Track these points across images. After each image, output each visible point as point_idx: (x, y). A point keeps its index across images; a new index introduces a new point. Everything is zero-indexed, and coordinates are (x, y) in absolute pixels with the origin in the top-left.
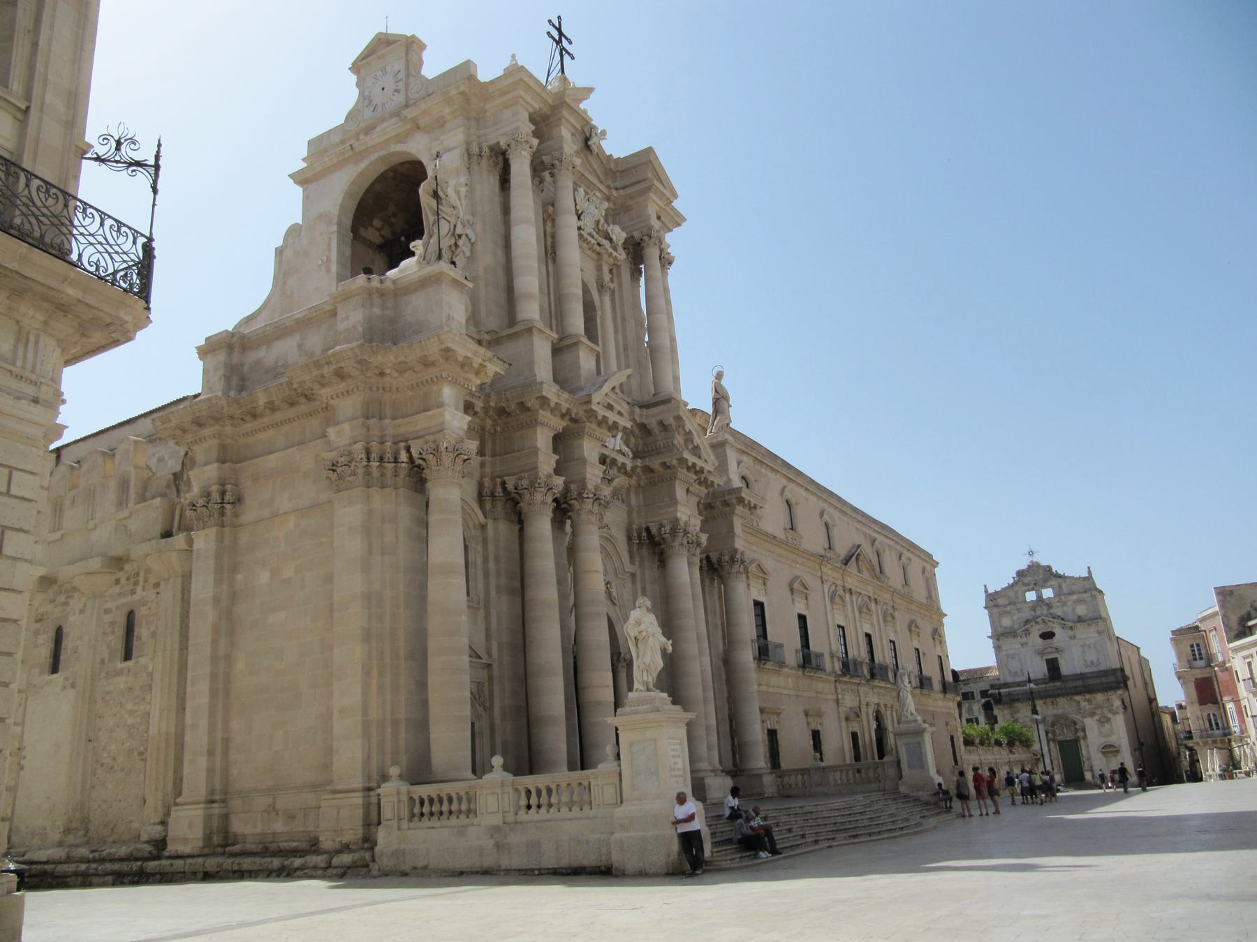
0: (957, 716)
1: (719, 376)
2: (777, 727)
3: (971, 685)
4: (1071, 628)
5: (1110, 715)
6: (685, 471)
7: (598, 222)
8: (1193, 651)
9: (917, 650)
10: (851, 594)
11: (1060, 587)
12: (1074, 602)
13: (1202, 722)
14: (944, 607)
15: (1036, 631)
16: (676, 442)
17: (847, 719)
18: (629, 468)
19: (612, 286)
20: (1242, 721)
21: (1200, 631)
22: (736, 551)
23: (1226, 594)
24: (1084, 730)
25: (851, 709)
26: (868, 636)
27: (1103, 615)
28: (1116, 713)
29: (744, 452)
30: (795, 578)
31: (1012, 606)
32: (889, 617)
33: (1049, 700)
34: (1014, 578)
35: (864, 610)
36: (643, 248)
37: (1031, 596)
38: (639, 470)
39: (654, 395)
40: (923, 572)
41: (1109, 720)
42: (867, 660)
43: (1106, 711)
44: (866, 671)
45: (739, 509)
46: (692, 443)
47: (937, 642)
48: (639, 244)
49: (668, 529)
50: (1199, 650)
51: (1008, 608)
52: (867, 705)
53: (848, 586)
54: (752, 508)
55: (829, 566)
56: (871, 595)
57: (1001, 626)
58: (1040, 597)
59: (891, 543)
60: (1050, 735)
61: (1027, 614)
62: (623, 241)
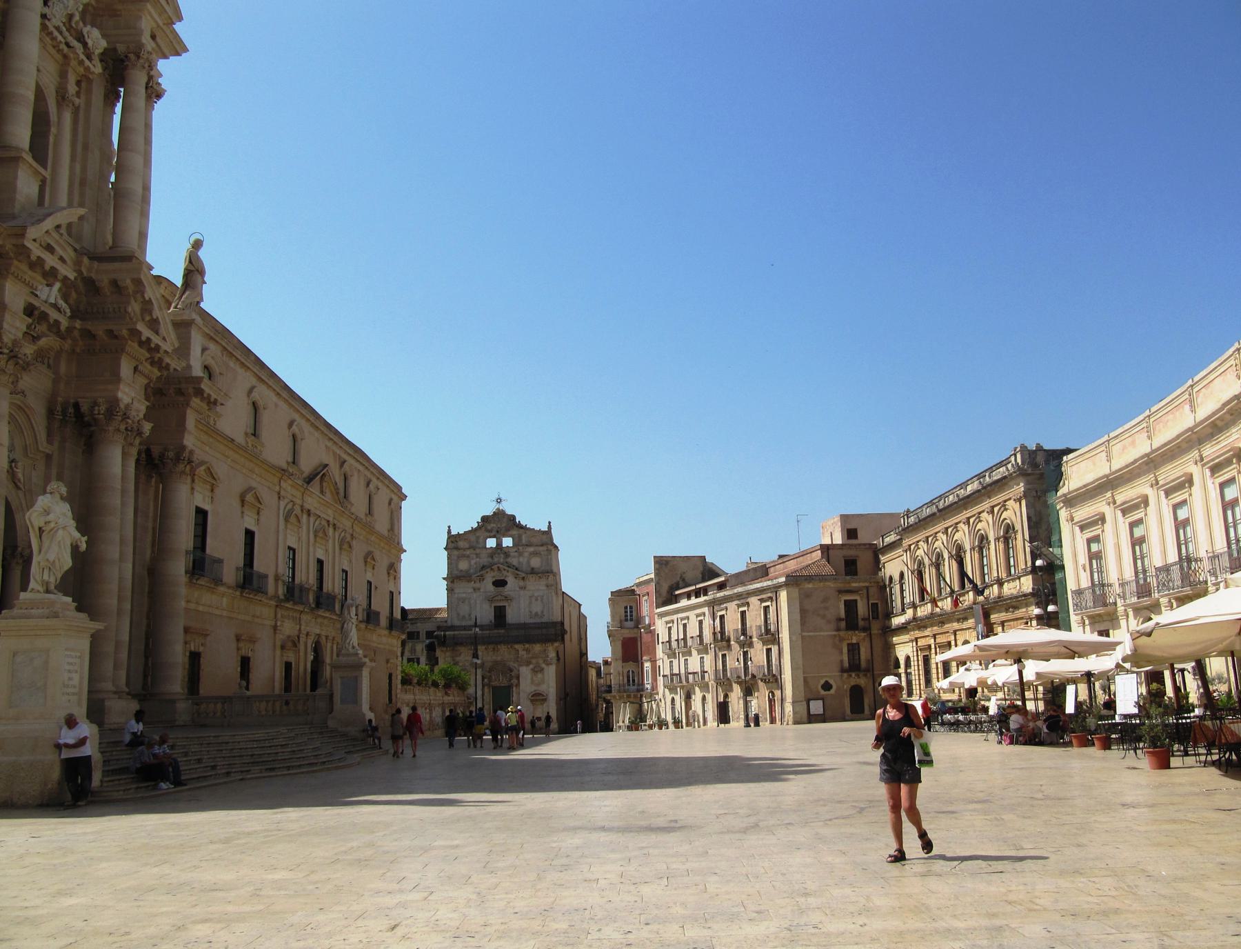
0: (399, 654)
1: (197, 245)
2: (201, 649)
3: (419, 624)
4: (523, 578)
5: (544, 666)
6: (136, 345)
7: (71, 17)
8: (626, 612)
9: (370, 583)
10: (309, 515)
11: (520, 536)
13: (621, 678)
14: (405, 543)
15: (490, 578)
16: (130, 309)
17: (283, 647)
18: (63, 328)
19: (77, 101)
20: (655, 679)
21: (635, 595)
22: (183, 448)
23: (662, 563)
24: (518, 678)
25: (289, 637)
26: (320, 563)
27: (555, 570)
28: (548, 664)
29: (211, 338)
30: (250, 489)
31: (472, 551)
32: (345, 544)
33: (491, 647)
34: (478, 522)
35: (320, 534)
36: (126, 68)
37: (491, 543)
38: (76, 333)
39: (110, 248)
40: (390, 504)
41: (542, 670)
42: (315, 588)
43: (541, 661)
44: (311, 598)
45: (196, 402)
46: (151, 314)
47: (392, 577)
48: (122, 61)
49: (103, 408)
50: (631, 612)
51: (468, 552)
52: (307, 634)
53: (307, 506)
54: (211, 403)
55: (290, 482)
56: (331, 519)
57: (457, 570)
58: (499, 544)
59: (361, 468)
60: (486, 680)
61: (485, 560)
62: (101, 51)
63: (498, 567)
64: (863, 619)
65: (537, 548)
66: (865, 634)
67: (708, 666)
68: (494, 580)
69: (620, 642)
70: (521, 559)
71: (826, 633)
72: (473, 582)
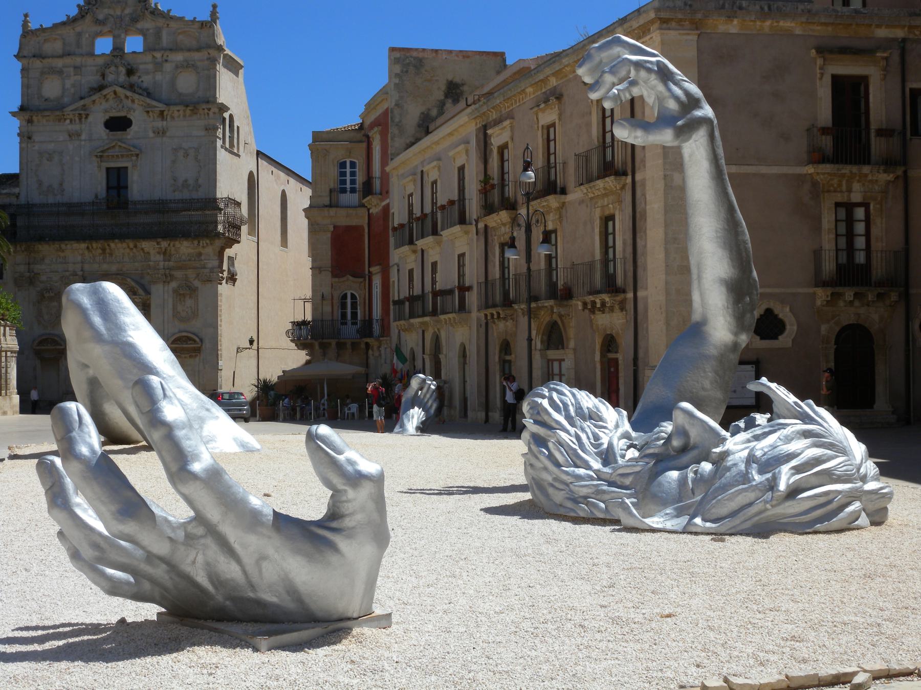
8: (343, 174)
12: (179, 67)
13: (328, 309)
15: (100, 112)
34: (78, 6)
50: (353, 174)
51: (59, 63)
58: (118, 49)
61: (90, 78)
63: (115, 93)
64: (880, 132)
65: (187, 54)
66: (891, 177)
67: (473, 275)
68: (107, 117)
69: (329, 235)
70: (159, 77)
71: (775, 170)
72: (68, 121)
